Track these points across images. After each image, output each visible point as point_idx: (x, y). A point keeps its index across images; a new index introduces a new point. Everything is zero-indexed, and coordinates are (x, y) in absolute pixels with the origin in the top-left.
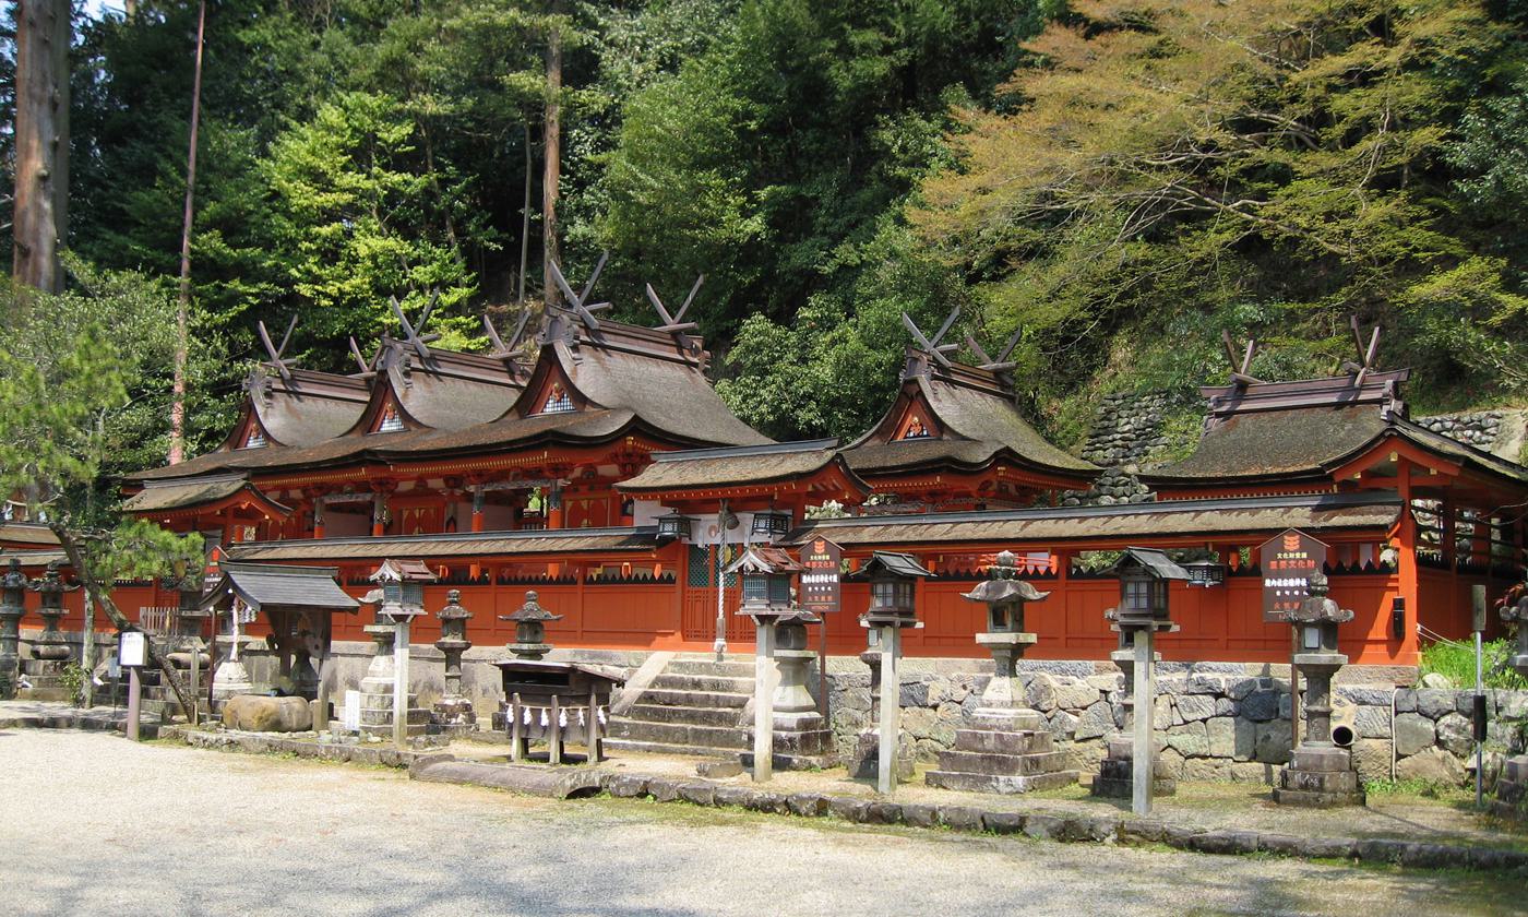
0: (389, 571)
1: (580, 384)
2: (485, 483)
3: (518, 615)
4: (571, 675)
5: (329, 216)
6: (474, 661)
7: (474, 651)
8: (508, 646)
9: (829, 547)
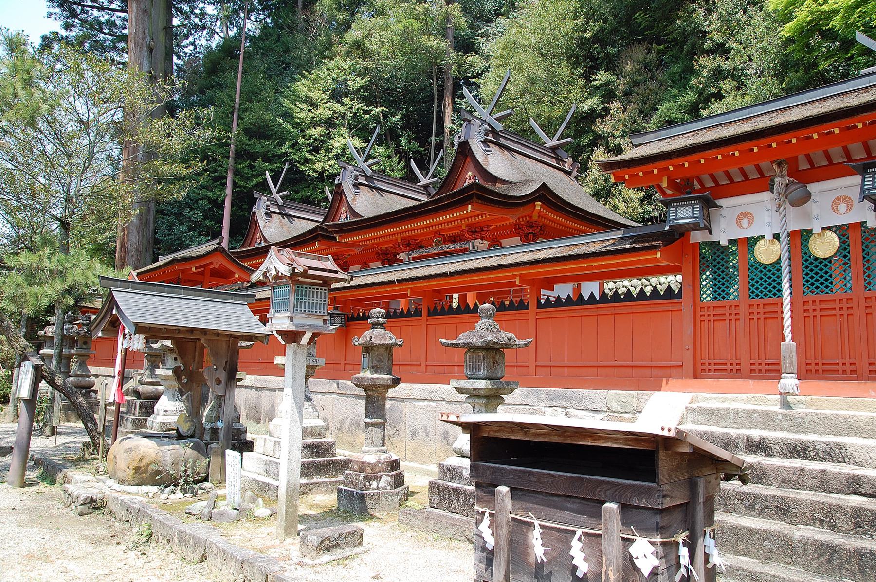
1: (491, 169)
2: (412, 250)
3: (464, 337)
4: (662, 455)
5: (314, 124)
6: (403, 400)
7: (402, 389)
8: (454, 383)
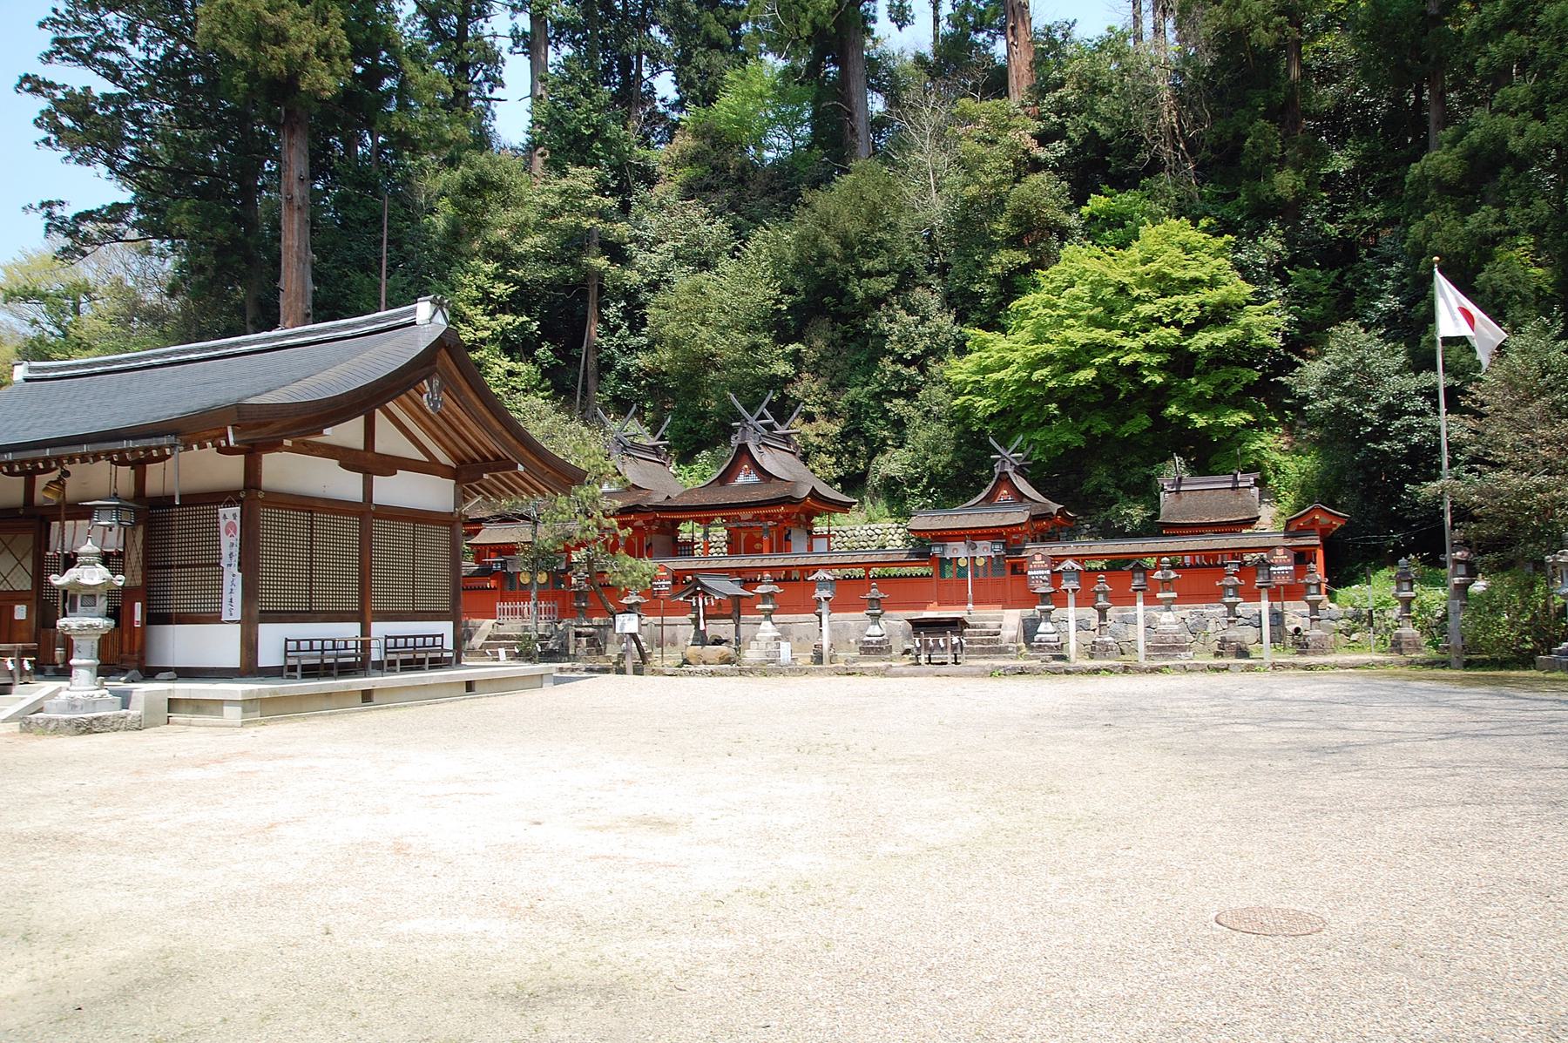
3: (868, 596)
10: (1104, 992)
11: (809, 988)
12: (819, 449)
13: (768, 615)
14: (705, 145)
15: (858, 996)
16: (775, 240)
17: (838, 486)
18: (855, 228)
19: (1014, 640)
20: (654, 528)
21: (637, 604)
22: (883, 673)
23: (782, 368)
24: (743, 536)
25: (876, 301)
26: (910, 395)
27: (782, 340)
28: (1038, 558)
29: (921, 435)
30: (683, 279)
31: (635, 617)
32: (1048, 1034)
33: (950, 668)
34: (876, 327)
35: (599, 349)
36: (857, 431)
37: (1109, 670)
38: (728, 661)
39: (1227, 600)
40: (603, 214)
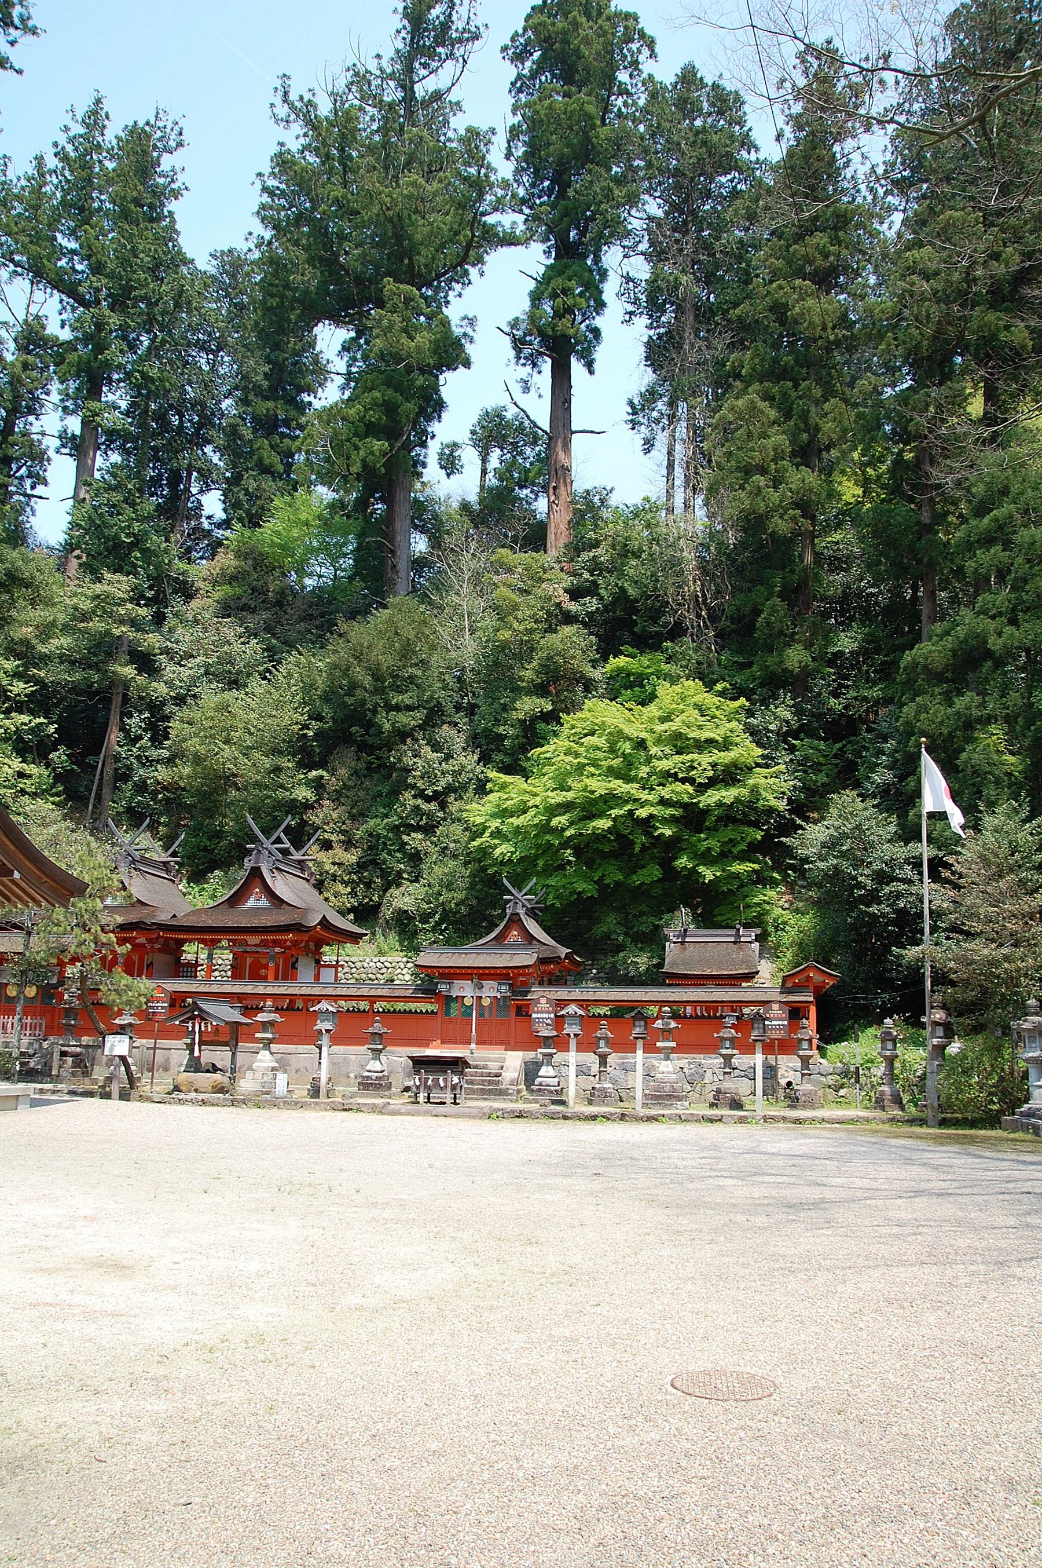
0: (324, 1005)
3: (371, 1030)
9: (549, 1001)
10: (549, 1462)
11: (243, 1457)
12: (334, 878)
13: (267, 1044)
14: (247, 565)
15: (293, 1466)
16: (308, 666)
17: (351, 916)
18: (387, 661)
19: (515, 1082)
20: (157, 946)
21: (130, 1025)
22: (381, 1110)
23: (303, 793)
24: (249, 961)
25: (403, 735)
26: (428, 830)
27: (306, 764)
28: (543, 1001)
29: (436, 871)
30: (210, 695)
31: (126, 1039)
32: (484, 1509)
33: (449, 1108)
34: (400, 760)
35: (117, 758)
36: (374, 863)
37: (606, 1117)
38: (221, 1090)
39: (724, 1052)
40: (135, 623)
